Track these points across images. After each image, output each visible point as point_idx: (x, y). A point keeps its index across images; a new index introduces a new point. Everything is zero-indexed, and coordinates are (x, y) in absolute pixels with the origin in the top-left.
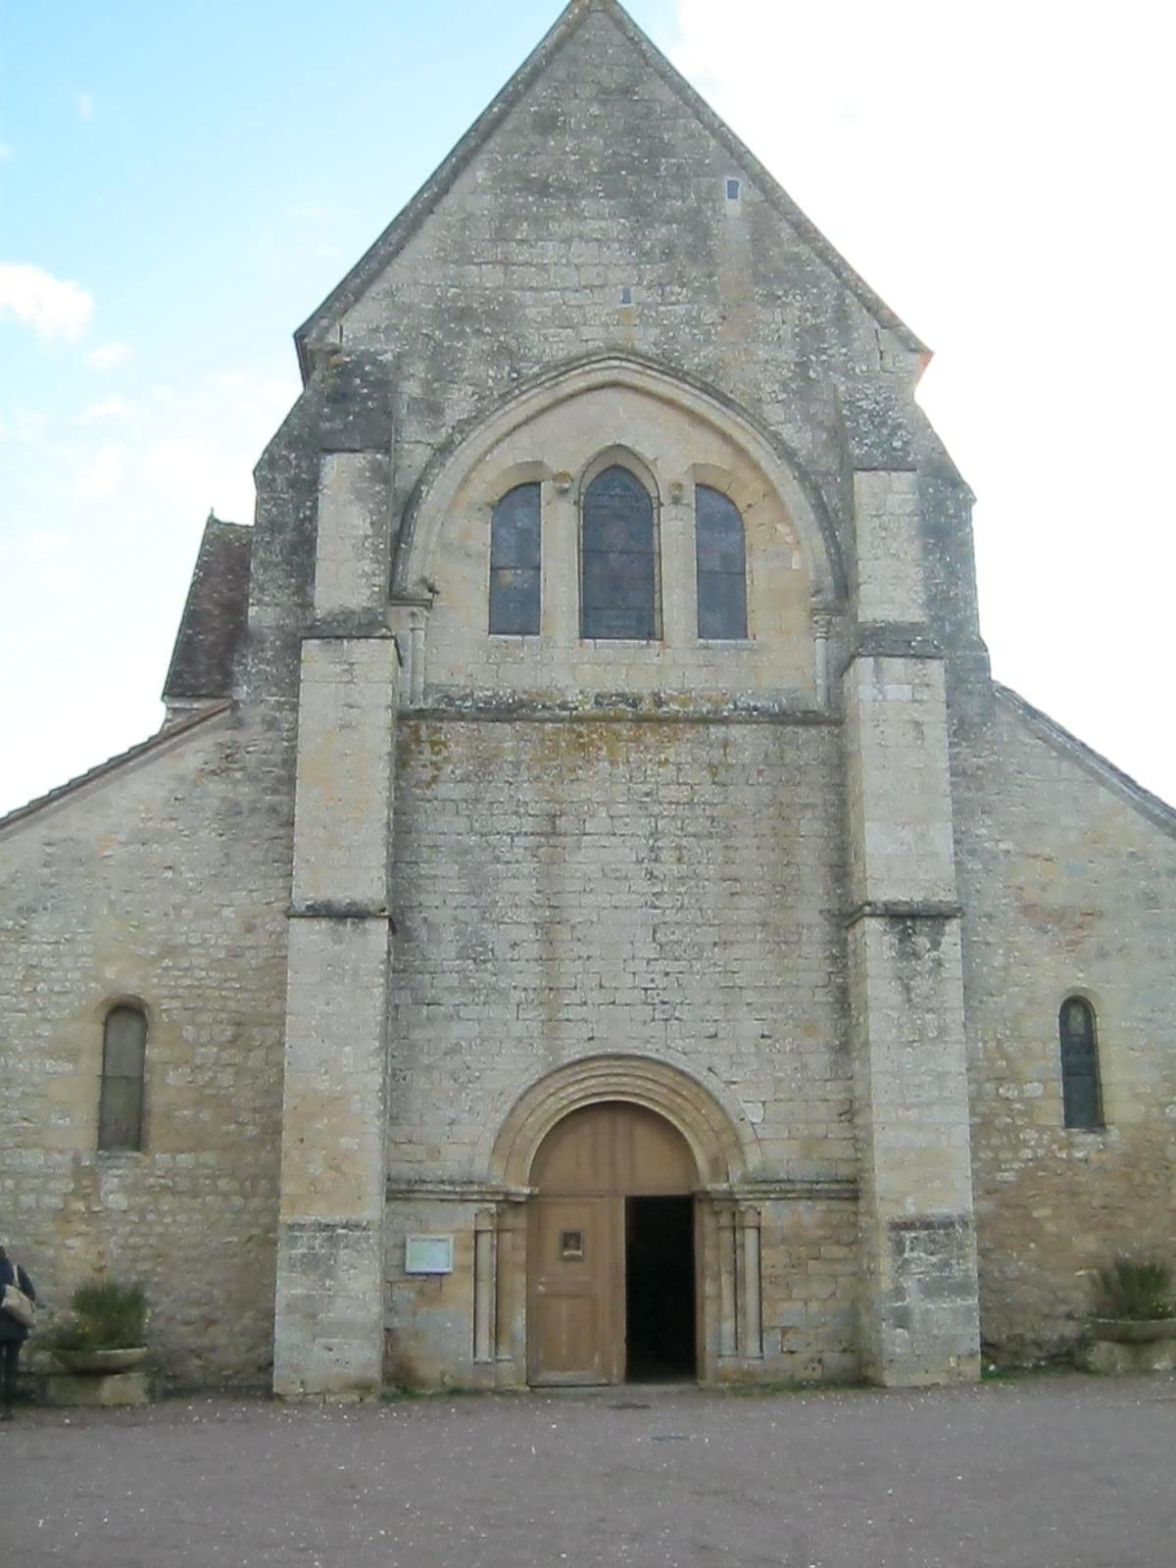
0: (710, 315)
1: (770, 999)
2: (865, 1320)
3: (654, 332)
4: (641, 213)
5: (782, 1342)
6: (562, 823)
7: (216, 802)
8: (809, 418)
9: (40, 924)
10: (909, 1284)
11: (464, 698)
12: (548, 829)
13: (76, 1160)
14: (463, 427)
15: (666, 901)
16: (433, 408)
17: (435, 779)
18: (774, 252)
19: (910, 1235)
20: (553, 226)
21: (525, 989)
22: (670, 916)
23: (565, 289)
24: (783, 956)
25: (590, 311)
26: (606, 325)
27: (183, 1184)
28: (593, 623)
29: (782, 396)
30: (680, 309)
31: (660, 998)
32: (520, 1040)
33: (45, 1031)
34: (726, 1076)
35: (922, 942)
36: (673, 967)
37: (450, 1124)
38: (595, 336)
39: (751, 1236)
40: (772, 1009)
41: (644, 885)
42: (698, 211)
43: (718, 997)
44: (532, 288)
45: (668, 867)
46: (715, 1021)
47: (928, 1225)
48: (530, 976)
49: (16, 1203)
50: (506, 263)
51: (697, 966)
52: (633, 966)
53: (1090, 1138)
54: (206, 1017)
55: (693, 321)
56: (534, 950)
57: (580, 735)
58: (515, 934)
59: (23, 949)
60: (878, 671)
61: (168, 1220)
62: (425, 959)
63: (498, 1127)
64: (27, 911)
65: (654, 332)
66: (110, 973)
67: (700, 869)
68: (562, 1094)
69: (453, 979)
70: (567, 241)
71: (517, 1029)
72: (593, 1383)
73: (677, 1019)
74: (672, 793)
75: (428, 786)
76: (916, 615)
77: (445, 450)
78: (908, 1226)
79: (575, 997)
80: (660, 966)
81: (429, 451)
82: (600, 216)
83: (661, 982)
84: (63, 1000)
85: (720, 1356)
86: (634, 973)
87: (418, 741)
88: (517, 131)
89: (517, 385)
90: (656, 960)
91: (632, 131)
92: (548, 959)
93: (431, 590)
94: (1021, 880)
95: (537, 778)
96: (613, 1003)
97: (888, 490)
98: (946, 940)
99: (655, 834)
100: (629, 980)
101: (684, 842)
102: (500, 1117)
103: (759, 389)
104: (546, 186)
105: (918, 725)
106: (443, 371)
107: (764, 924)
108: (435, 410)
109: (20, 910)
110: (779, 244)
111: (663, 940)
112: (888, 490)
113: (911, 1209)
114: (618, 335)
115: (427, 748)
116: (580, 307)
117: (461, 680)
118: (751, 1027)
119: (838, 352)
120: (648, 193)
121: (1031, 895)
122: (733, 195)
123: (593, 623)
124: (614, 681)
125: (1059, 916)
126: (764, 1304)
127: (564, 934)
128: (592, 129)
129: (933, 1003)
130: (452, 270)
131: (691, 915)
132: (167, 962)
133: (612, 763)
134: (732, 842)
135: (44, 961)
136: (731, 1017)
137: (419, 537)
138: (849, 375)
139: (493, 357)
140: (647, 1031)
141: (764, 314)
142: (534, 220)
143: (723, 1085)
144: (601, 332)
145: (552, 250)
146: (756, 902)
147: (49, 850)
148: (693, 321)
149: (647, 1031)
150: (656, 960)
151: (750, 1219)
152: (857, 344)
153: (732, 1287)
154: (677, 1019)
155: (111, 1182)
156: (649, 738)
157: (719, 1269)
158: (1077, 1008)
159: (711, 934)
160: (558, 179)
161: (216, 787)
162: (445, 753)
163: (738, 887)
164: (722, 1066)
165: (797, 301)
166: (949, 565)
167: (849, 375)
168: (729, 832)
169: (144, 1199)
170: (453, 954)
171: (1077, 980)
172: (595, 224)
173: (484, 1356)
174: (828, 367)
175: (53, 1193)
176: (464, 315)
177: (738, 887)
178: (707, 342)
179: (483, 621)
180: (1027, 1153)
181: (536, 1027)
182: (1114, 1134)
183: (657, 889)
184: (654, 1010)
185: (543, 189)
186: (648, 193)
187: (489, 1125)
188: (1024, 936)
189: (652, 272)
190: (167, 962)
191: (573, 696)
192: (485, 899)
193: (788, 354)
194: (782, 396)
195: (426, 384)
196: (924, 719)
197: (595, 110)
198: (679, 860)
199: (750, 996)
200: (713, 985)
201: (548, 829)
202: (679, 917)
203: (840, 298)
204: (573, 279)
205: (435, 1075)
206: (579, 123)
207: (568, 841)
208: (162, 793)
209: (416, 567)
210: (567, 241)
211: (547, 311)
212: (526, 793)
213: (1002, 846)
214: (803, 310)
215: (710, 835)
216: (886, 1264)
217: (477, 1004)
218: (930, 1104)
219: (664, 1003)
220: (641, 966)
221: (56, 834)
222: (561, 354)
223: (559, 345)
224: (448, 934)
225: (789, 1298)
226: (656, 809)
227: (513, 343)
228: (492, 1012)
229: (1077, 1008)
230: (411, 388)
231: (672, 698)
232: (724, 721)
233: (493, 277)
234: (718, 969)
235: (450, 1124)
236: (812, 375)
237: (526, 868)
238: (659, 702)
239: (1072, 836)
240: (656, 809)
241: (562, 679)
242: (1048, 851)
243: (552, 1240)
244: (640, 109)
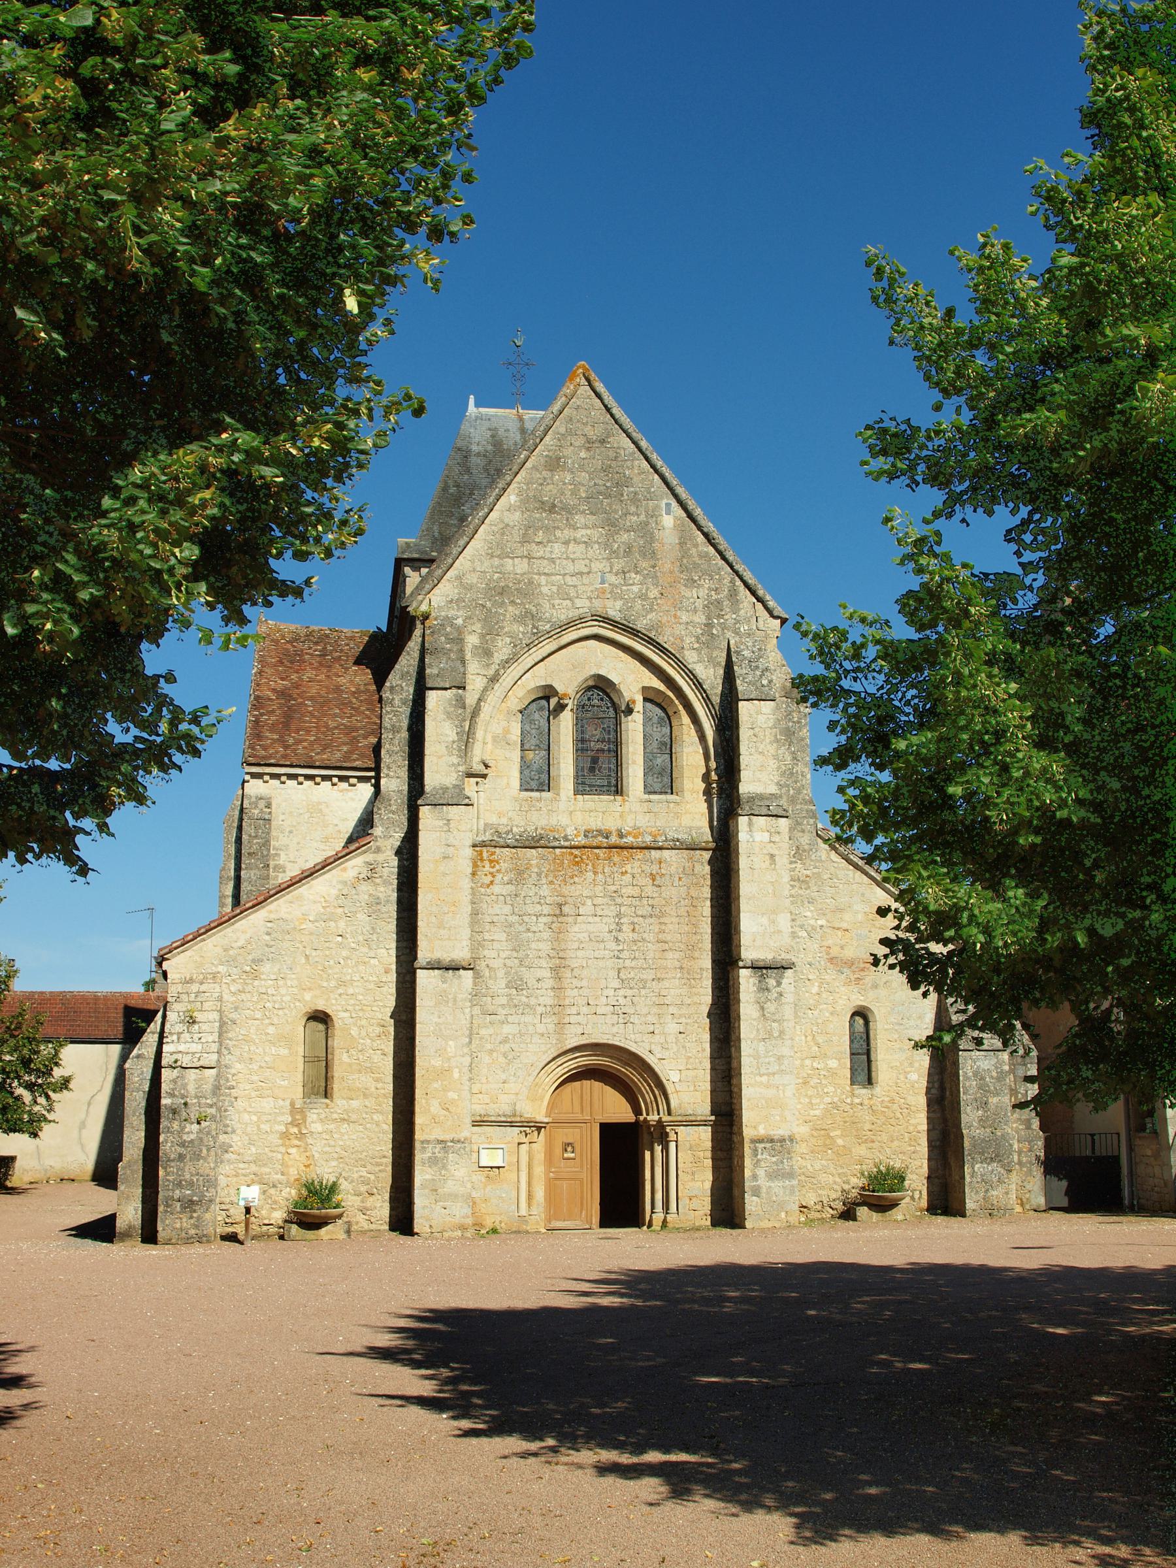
0: (654, 593)
1: (684, 1011)
2: (736, 1192)
3: (619, 604)
4: (612, 525)
6: (566, 909)
7: (366, 897)
8: (711, 660)
9: (266, 968)
10: (761, 1173)
11: (507, 833)
12: (558, 912)
13: (292, 1104)
14: (507, 663)
15: (625, 955)
16: (486, 652)
17: (492, 882)
18: (693, 551)
19: (760, 1146)
20: (558, 533)
22: (628, 963)
23: (565, 575)
24: (691, 987)
25: (581, 589)
26: (590, 598)
27: (354, 1117)
28: (583, 786)
29: (696, 646)
30: (635, 589)
33: (271, 1030)
35: (772, 982)
36: (629, 993)
38: (583, 606)
39: (672, 1145)
41: (613, 945)
42: (647, 524)
43: (655, 1010)
44: (545, 574)
45: (627, 934)
47: (772, 1141)
48: (548, 999)
49: (259, 1128)
50: (529, 557)
51: (643, 992)
52: (606, 992)
53: (864, 1091)
54: (364, 1022)
55: (643, 597)
56: (549, 983)
57: (576, 857)
58: (541, 973)
59: (256, 983)
60: (750, 824)
61: (346, 1137)
62: (488, 988)
64: (257, 961)
65: (619, 604)
66: (308, 996)
67: (645, 936)
69: (503, 1000)
70: (566, 543)
71: (541, 1028)
74: (628, 891)
75: (488, 886)
76: (773, 789)
77: (494, 679)
78: (761, 1141)
79: (574, 1010)
80: (622, 992)
81: (485, 680)
82: (586, 527)
83: (622, 1001)
84: (281, 1012)
87: (482, 860)
88: (534, 468)
89: (538, 637)
91: (605, 470)
92: (558, 989)
93: (487, 766)
94: (830, 942)
95: (551, 882)
97: (759, 712)
98: (785, 981)
99: (619, 915)
100: (604, 1000)
101: (636, 920)
103: (682, 640)
104: (554, 506)
105: (772, 856)
106: (491, 631)
107: (681, 968)
108: (488, 653)
109: (253, 961)
110: (696, 546)
111: (624, 977)
112: (759, 712)
113: (762, 1131)
114: (598, 606)
115: (487, 864)
116: (575, 586)
117: (504, 821)
118: (672, 1028)
119: (730, 617)
120: (616, 512)
121: (835, 951)
122: (668, 513)
123: (583, 786)
124: (595, 823)
125: (850, 963)
127: (567, 974)
128: (582, 468)
129: (777, 1017)
130: (496, 561)
131: (641, 962)
132: (340, 991)
133: (595, 873)
134: (662, 920)
135: (270, 992)
137: (479, 734)
138: (737, 632)
139: (521, 619)
140: (615, 1030)
141: (688, 593)
142: (547, 529)
144: (588, 604)
145: (557, 549)
146: (677, 955)
147: (269, 925)
148: (643, 597)
149: (615, 1030)
151: (672, 1136)
152: (742, 612)
155: (312, 1116)
156: (616, 859)
158: (862, 1014)
159: (648, 975)
160: (561, 502)
161: (365, 887)
162: (497, 867)
163: (666, 946)
164: (657, 1050)
165: (707, 584)
166: (793, 753)
167: (737, 632)
168: (663, 914)
169: (332, 1126)
171: (859, 1001)
172: (584, 532)
173: (523, 1212)
174: (724, 627)
175: (279, 1123)
176: (503, 591)
177: (666, 946)
178: (652, 610)
179: (516, 783)
180: (829, 1100)
181: (551, 1027)
182: (878, 1090)
183: (621, 948)
185: (552, 509)
186: (616, 512)
188: (830, 975)
189: (618, 565)
190: (340, 991)
191: (570, 831)
192: (521, 954)
193: (700, 618)
194: (696, 646)
195: (482, 636)
196: (775, 852)
197: (583, 454)
198: (633, 930)
199: (672, 1009)
201: (558, 912)
202: (634, 963)
203: (732, 582)
204: (570, 568)
205: (495, 1054)
206: (573, 463)
207: (570, 919)
208: (334, 892)
209: (478, 753)
210: (566, 543)
211: (554, 589)
212: (545, 891)
213: (820, 922)
214: (710, 589)
215: (651, 916)
216: (748, 1162)
218: (774, 1074)
220: (611, 992)
221: (272, 916)
222: (563, 617)
223: (563, 613)
224: (501, 973)
225: (693, 1180)
226: (619, 900)
227: (534, 609)
228: (528, 1019)
229: (862, 1014)
230: (472, 640)
231: (629, 833)
232: (660, 848)
233: (521, 566)
236: (715, 632)
237: (546, 935)
238: (621, 836)
239: (860, 917)
240: (619, 900)
241: (564, 820)
242: (845, 925)
243: (558, 1150)
244: (611, 454)
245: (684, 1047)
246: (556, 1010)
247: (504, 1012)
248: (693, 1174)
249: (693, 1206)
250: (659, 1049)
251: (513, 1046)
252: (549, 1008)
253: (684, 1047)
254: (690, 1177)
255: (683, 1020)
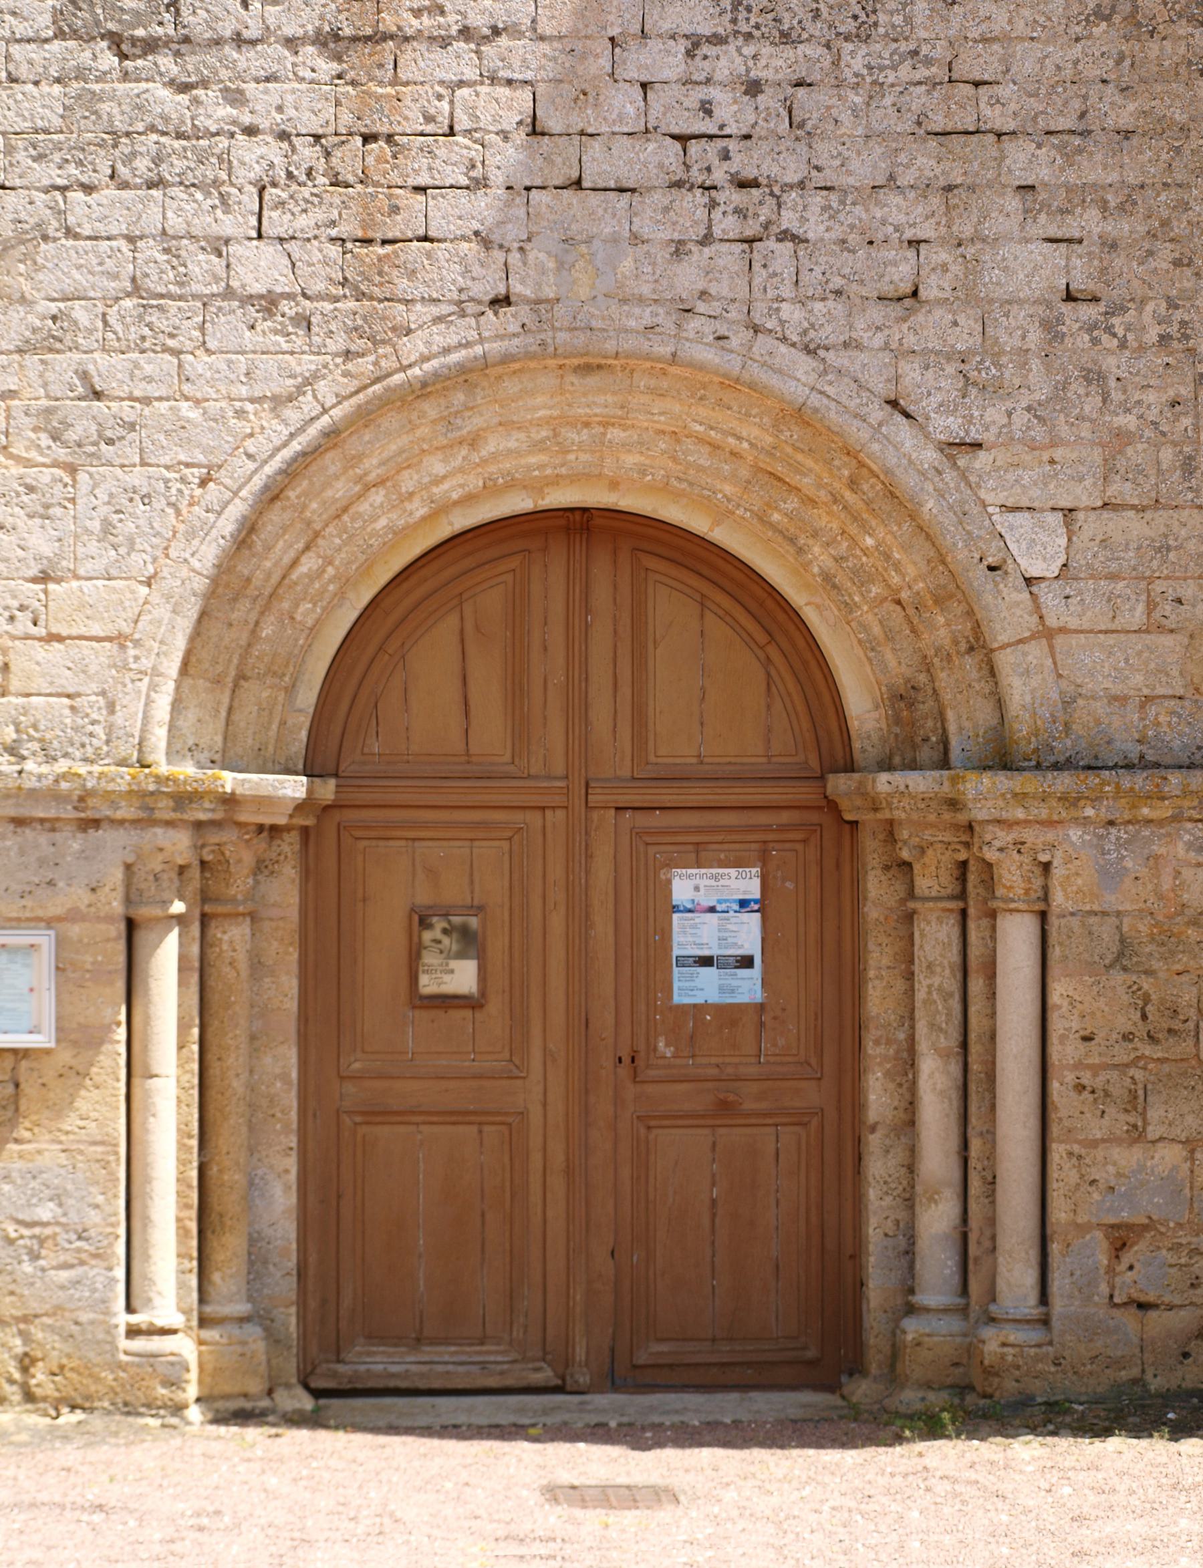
5: (1111, 1271)
21: (283, 136)
31: (734, 166)
32: (269, 303)
34: (947, 426)
37: (44, 578)
40: (1104, 206)
46: (915, 243)
51: (856, 59)
63: (200, 584)
68: (408, 481)
72: (509, 1382)
73: (785, 236)
85: (911, 1310)
86: (644, 86)
90: (717, 40)
96: (578, 184)
102: (208, 554)
126: (1057, 1152)
136: (968, 231)
143: (930, 455)
150: (717, 40)
153: (955, 1095)
154: (785, 236)
157: (912, 1039)
170: (44, 23)
184: (713, 205)
187: (170, 583)
200: (909, 126)
217: (124, 186)
219: (743, 184)
225: (1136, 1135)
234: (922, 73)
235: (44, 578)
245: (1094, 377)
246: (349, 158)
247: (50, 174)
248: (1135, 1101)
249: (1129, 1283)
250: (947, 383)
251: (101, 364)
252: (308, 153)
253: (1094, 377)
254: (1117, 1121)
255: (1088, 222)
